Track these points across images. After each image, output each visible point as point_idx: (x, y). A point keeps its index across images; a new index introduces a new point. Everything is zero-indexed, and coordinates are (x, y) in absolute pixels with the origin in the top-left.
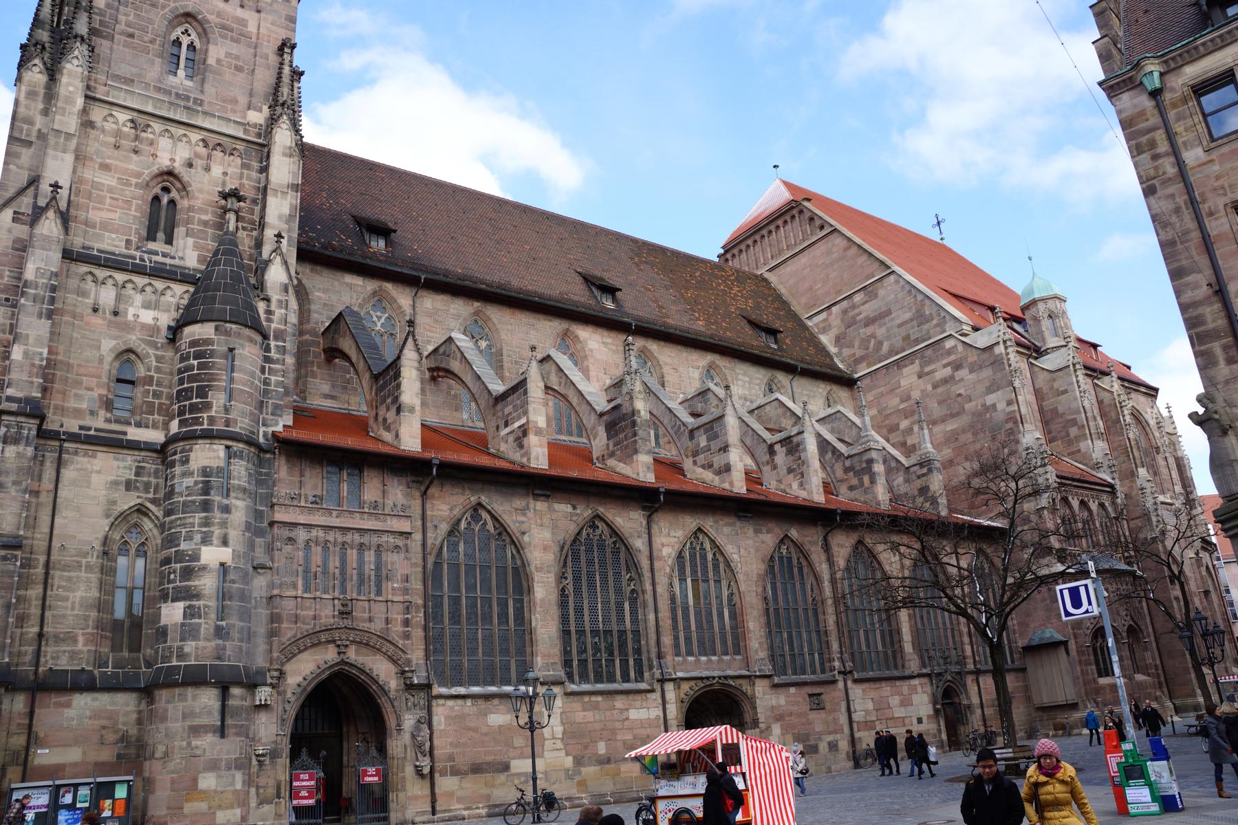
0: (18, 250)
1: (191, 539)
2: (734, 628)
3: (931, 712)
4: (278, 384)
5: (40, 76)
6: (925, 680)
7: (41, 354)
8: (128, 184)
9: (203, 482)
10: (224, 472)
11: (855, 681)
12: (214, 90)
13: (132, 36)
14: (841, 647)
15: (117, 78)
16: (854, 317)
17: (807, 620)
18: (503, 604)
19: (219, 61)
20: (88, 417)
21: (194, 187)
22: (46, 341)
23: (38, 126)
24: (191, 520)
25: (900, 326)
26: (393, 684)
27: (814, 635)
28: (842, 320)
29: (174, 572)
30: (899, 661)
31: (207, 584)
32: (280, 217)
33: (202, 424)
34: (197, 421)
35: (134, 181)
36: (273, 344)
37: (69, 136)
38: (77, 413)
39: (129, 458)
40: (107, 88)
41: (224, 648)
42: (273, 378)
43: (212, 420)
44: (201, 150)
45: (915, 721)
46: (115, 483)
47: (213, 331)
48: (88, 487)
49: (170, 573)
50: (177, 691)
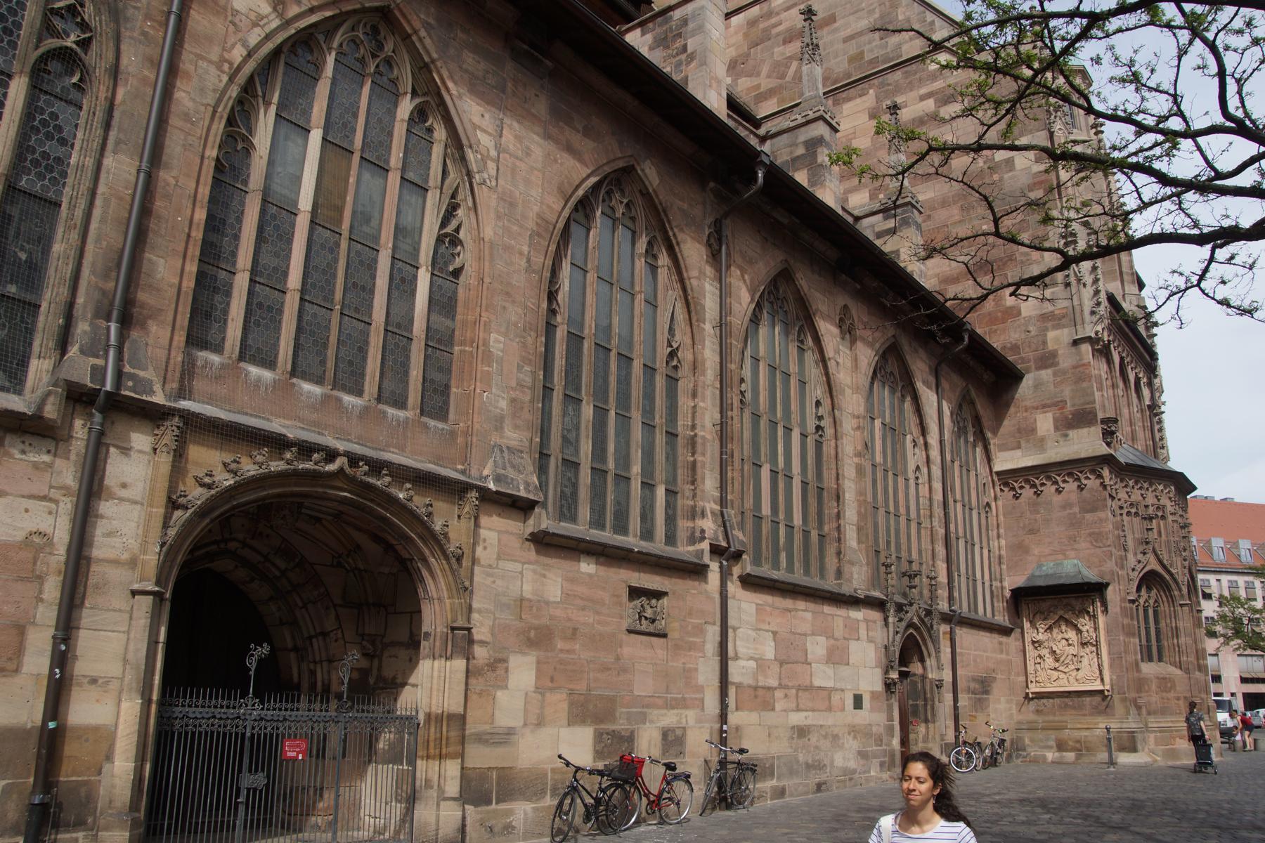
2: (439, 342)
3: (879, 687)
6: (875, 615)
11: (749, 582)
14: (723, 486)
16: (765, 30)
17: (649, 396)
25: (847, 40)
27: (660, 439)
28: (746, 35)
30: (831, 562)
45: (850, 702)
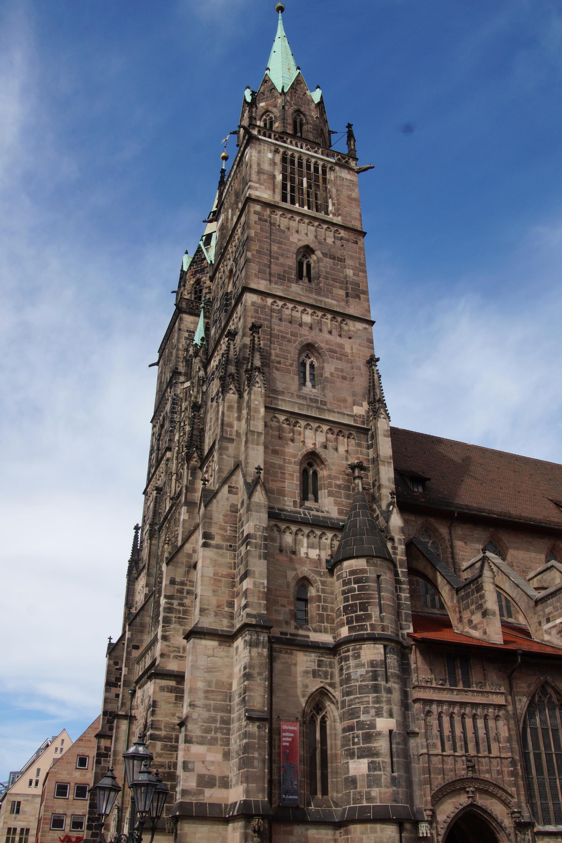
0: (233, 512)
1: (368, 712)
4: (406, 599)
5: (233, 395)
7: (263, 584)
9: (372, 671)
12: (331, 394)
20: (284, 626)
21: (329, 461)
22: (265, 575)
23: (235, 428)
24: (366, 699)
29: (358, 737)
32: (389, 480)
33: (367, 630)
34: (362, 628)
35: (293, 460)
36: (399, 570)
37: (259, 434)
38: (278, 623)
39: (313, 655)
40: (270, 399)
41: (398, 794)
42: (403, 595)
43: (373, 627)
46: (306, 672)
47: (365, 563)
48: (290, 675)
49: (353, 738)
50: (369, 826)
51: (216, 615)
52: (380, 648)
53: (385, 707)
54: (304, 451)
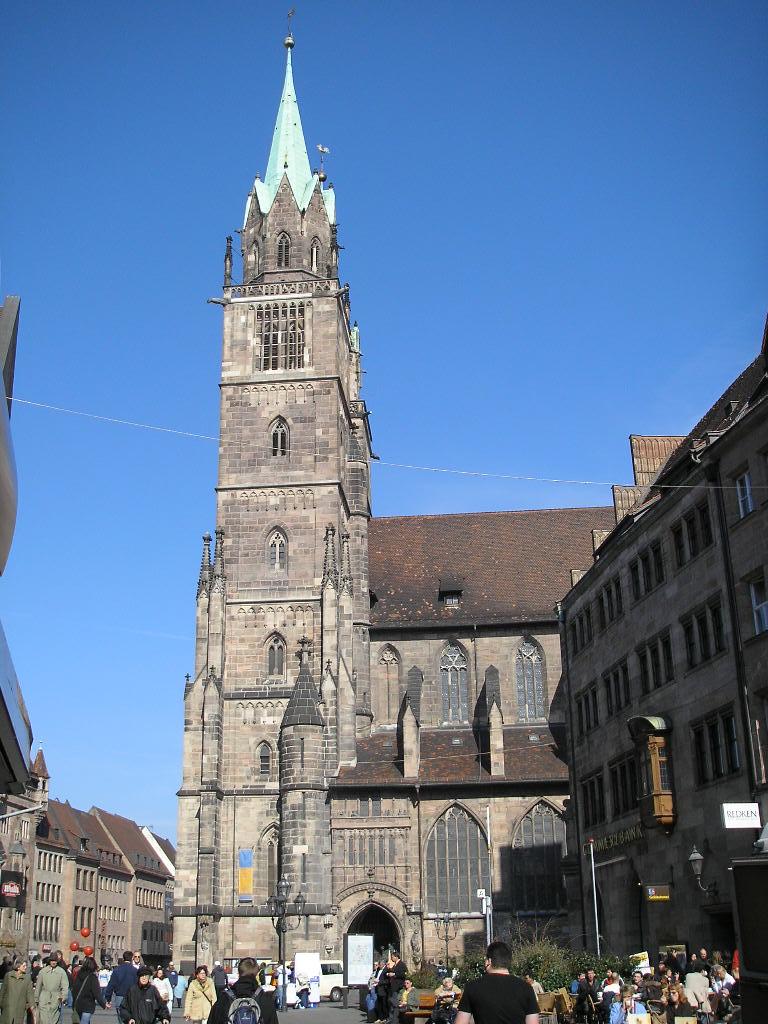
8: (254, 646)
10: (303, 806)
13: (247, 555)
15: (243, 584)
18: (474, 863)
19: (294, 551)
26: (401, 912)
31: (297, 864)
35: (257, 643)
43: (295, 779)
44: (291, 613)
46: (262, 813)
51: (195, 780)
52: (299, 793)
53: (300, 838)
54: (267, 634)
